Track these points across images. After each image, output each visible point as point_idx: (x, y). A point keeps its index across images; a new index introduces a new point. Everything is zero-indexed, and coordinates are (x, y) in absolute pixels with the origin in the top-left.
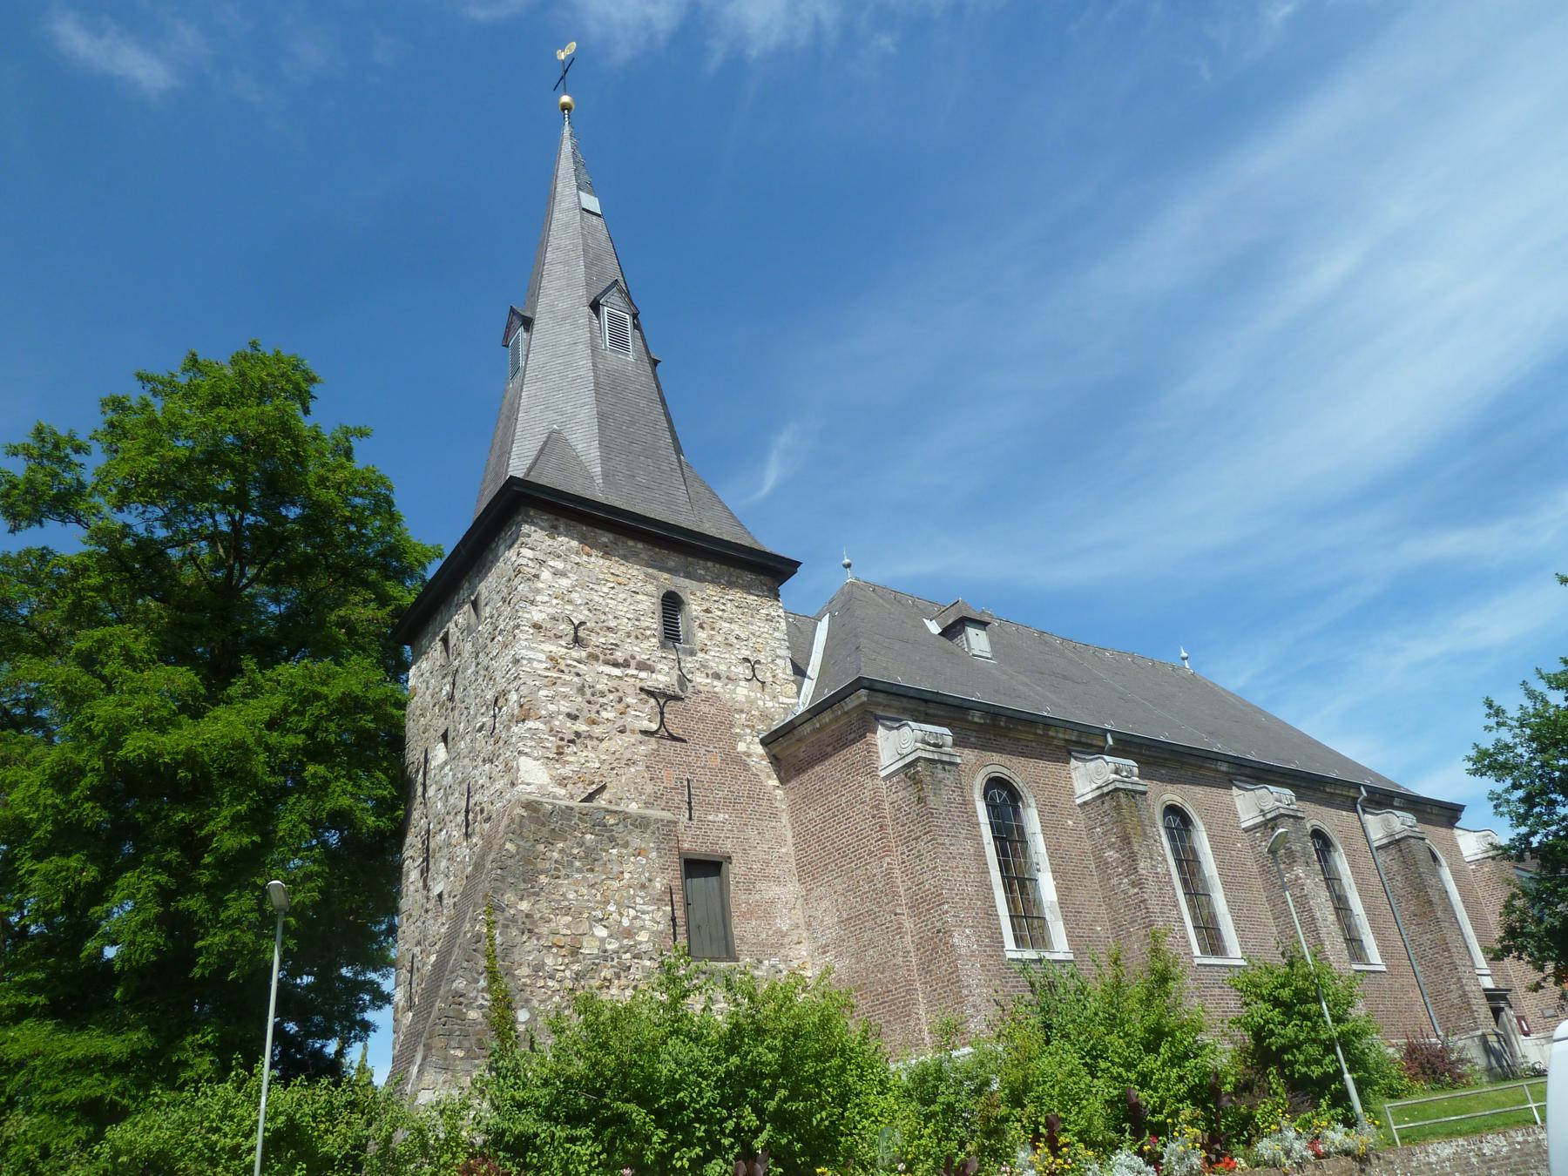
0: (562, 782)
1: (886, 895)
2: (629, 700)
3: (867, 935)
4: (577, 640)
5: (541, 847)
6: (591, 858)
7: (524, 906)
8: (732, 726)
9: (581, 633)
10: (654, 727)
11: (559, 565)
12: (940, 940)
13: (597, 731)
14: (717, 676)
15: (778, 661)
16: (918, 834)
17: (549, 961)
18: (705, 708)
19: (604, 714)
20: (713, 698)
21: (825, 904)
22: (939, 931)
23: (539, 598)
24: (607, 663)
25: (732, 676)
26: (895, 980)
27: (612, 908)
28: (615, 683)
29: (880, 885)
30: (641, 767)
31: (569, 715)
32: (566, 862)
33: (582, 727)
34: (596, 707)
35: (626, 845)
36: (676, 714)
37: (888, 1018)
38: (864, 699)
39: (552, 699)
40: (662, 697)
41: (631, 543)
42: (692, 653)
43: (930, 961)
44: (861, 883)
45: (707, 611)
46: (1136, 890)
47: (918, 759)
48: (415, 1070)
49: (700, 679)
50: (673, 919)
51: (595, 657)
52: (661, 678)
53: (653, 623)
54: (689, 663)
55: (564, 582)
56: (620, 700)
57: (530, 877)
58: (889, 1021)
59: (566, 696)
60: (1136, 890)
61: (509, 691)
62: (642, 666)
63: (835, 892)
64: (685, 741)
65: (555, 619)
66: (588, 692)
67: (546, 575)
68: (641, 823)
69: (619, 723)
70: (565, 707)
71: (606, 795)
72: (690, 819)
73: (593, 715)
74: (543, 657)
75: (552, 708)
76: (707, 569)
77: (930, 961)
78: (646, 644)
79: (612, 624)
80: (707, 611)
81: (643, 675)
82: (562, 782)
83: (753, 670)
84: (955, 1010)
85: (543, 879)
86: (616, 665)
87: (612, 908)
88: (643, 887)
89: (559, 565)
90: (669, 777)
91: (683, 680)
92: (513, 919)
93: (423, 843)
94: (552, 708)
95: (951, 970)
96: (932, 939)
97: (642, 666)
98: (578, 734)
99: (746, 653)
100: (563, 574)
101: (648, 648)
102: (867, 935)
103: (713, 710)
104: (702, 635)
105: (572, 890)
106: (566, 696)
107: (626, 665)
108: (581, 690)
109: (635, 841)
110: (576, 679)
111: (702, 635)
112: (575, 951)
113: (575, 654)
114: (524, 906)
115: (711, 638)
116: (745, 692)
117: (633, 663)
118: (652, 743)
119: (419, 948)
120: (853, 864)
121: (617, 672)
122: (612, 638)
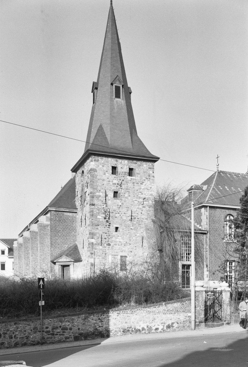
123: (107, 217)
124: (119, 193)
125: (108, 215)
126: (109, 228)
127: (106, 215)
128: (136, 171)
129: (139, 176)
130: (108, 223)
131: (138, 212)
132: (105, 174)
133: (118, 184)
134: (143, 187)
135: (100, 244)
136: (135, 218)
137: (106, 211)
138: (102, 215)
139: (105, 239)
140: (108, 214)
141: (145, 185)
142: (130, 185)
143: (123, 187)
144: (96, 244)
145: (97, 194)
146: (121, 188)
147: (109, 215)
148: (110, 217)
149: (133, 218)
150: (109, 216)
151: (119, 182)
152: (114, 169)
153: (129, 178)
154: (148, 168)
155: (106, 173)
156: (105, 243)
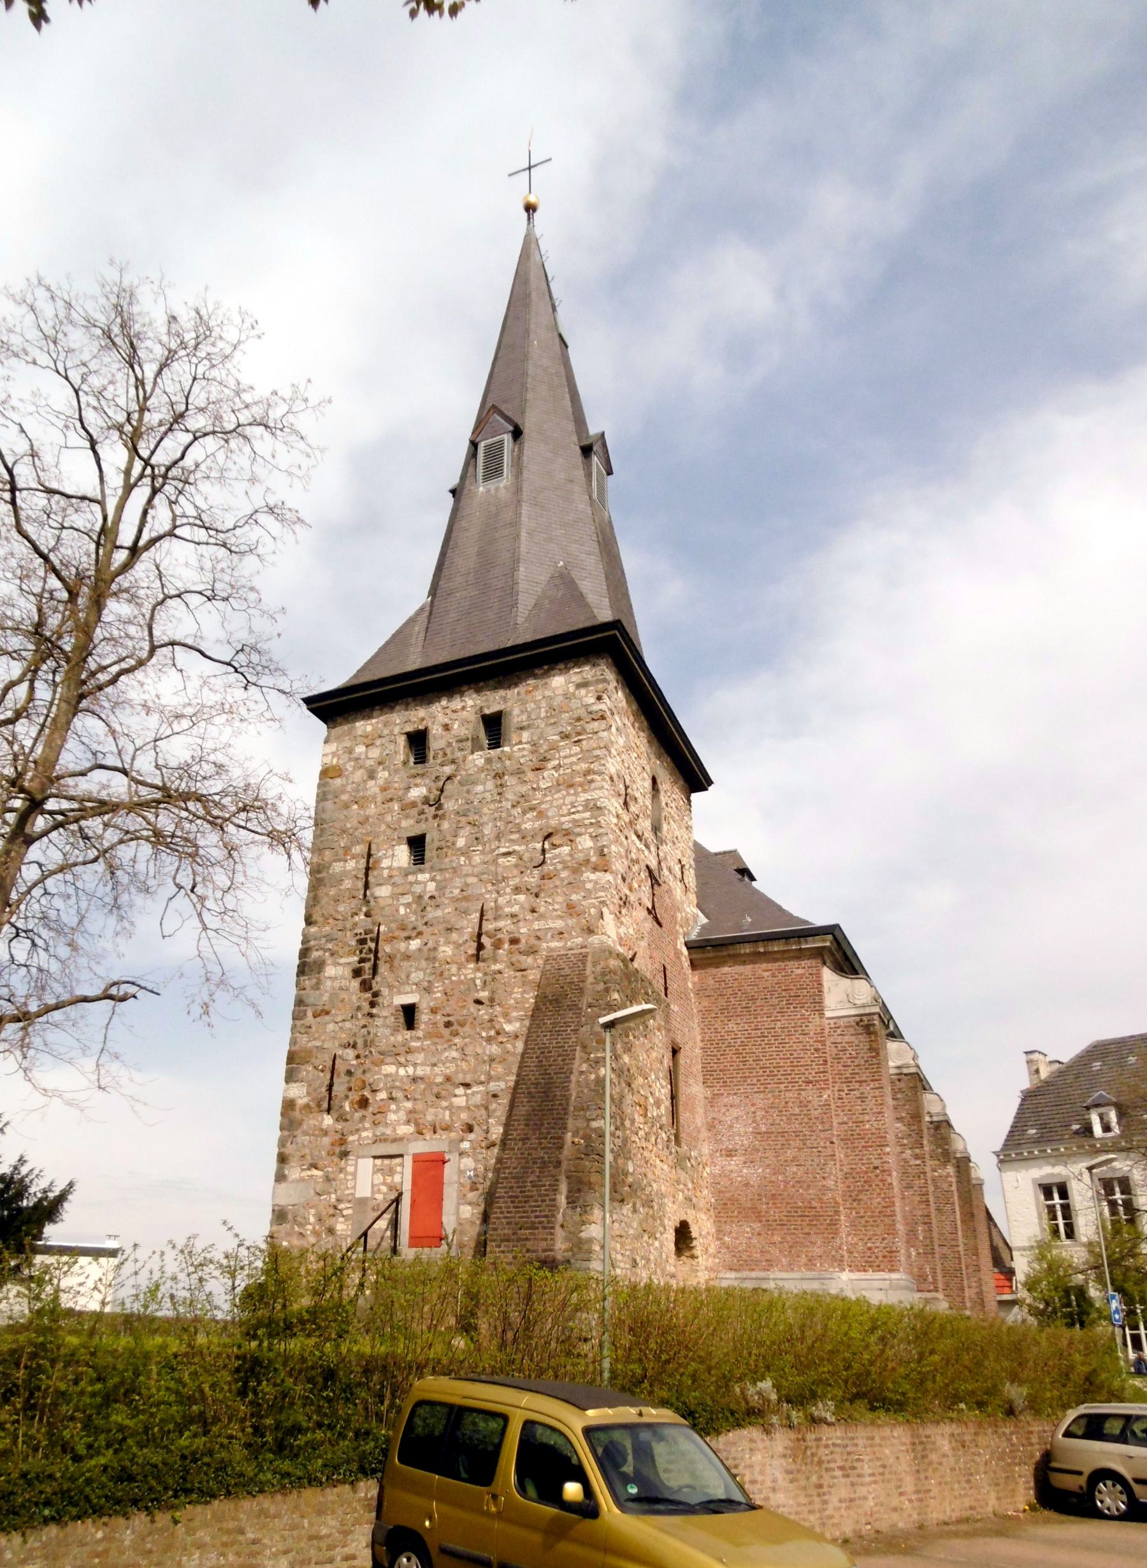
1: (823, 1123)
3: (790, 1154)
12: (877, 1176)
16: (864, 1078)
21: (735, 1112)
22: (876, 1168)
26: (820, 1199)
29: (816, 1112)
37: (806, 1230)
38: (828, 944)
43: (860, 1191)
44: (790, 1104)
46: (918, 1162)
47: (874, 1014)
48: (562, 1199)
58: (809, 1234)
60: (918, 1162)
61: (580, 835)
63: (753, 1105)
64: (660, 925)
77: (860, 1191)
84: (884, 1239)
93: (362, 942)
95: (884, 1204)
96: (866, 1172)
102: (790, 1154)
119: (350, 1053)
120: (782, 1086)
123: (367, 966)
124: (428, 839)
125: (372, 956)
126: (371, 1015)
127: (363, 955)
128: (516, 716)
129: (525, 736)
130: (368, 995)
131: (515, 909)
132: (372, 775)
133: (426, 801)
134: (549, 776)
135: (325, 1105)
136: (497, 945)
137: (363, 936)
138: (342, 961)
139: (349, 1073)
140: (370, 950)
141: (557, 768)
142: (485, 788)
143: (449, 805)
144: (307, 1106)
145: (337, 867)
146: (440, 812)
147: (376, 952)
148: (380, 963)
149: (485, 940)
150: (376, 958)
151: (430, 791)
152: (418, 741)
153: (478, 759)
154: (572, 689)
155: (381, 767)
156: (347, 1097)
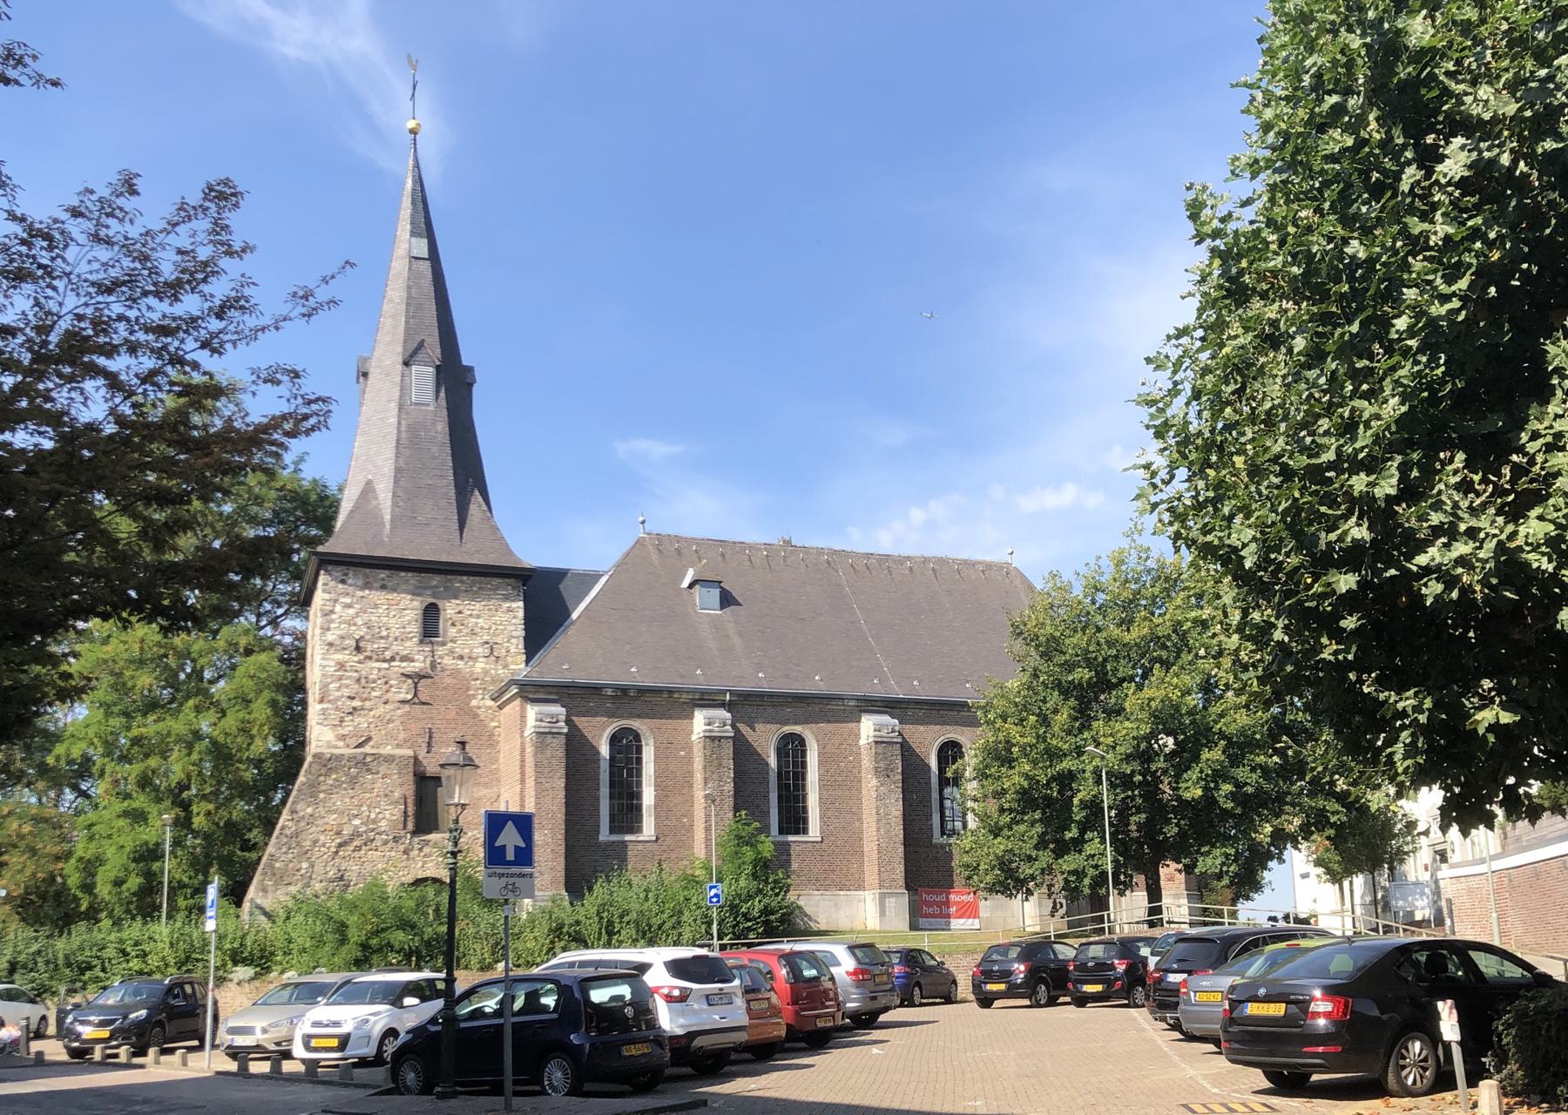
0: (343, 737)
2: (392, 682)
4: (358, 649)
5: (322, 778)
6: (353, 782)
7: (309, 810)
8: (468, 689)
9: (361, 645)
10: (409, 697)
11: (348, 600)
13: (368, 704)
14: (461, 658)
15: (513, 641)
17: (322, 838)
18: (448, 680)
19: (374, 694)
20: (456, 673)
23: (332, 625)
24: (377, 661)
25: (474, 655)
27: (364, 808)
28: (382, 673)
30: (397, 723)
31: (349, 697)
32: (338, 784)
33: (356, 703)
34: (368, 690)
35: (378, 773)
36: (426, 686)
39: (338, 689)
40: (417, 678)
41: (403, 574)
42: (444, 644)
45: (460, 612)
49: (448, 661)
50: (405, 812)
51: (370, 658)
52: (417, 664)
53: (415, 629)
54: (440, 651)
55: (351, 611)
56: (386, 683)
57: (314, 795)
59: (347, 686)
62: (404, 659)
65: (342, 637)
66: (363, 681)
67: (338, 608)
68: (389, 759)
69: (385, 697)
70: (346, 692)
71: (371, 743)
72: (428, 752)
73: (365, 696)
74: (333, 663)
75: (337, 694)
76: (462, 582)
78: (408, 644)
79: (384, 633)
80: (460, 612)
81: (404, 664)
82: (343, 737)
83: (492, 649)
85: (322, 796)
86: (384, 661)
87: (364, 808)
88: (386, 795)
89: (348, 600)
90: (416, 728)
91: (433, 665)
92: (303, 817)
94: (337, 694)
97: (404, 659)
98: (354, 709)
99: (486, 638)
100: (349, 606)
101: (411, 646)
103: (455, 681)
104: (452, 631)
105: (339, 801)
106: (347, 686)
107: (393, 659)
108: (358, 680)
109: (383, 769)
110: (355, 674)
111: (452, 631)
112: (339, 833)
113: (356, 659)
114: (309, 810)
115: (460, 631)
116: (482, 665)
117: (398, 658)
118: (407, 708)
121: (385, 665)
122: (382, 644)
